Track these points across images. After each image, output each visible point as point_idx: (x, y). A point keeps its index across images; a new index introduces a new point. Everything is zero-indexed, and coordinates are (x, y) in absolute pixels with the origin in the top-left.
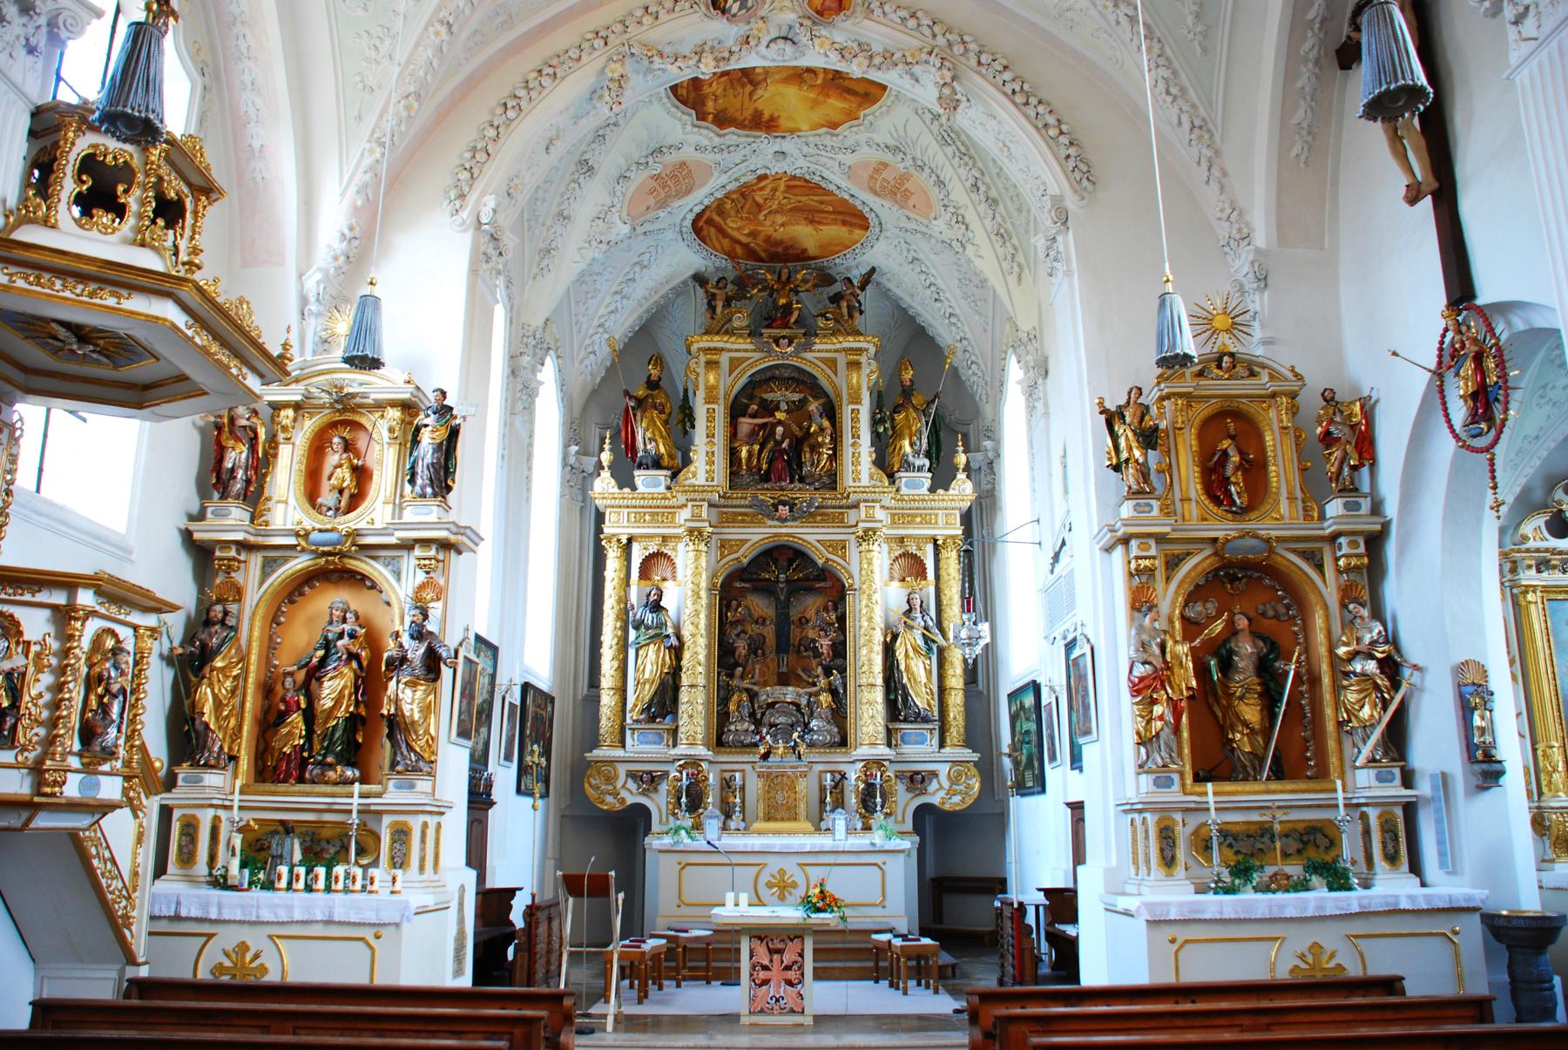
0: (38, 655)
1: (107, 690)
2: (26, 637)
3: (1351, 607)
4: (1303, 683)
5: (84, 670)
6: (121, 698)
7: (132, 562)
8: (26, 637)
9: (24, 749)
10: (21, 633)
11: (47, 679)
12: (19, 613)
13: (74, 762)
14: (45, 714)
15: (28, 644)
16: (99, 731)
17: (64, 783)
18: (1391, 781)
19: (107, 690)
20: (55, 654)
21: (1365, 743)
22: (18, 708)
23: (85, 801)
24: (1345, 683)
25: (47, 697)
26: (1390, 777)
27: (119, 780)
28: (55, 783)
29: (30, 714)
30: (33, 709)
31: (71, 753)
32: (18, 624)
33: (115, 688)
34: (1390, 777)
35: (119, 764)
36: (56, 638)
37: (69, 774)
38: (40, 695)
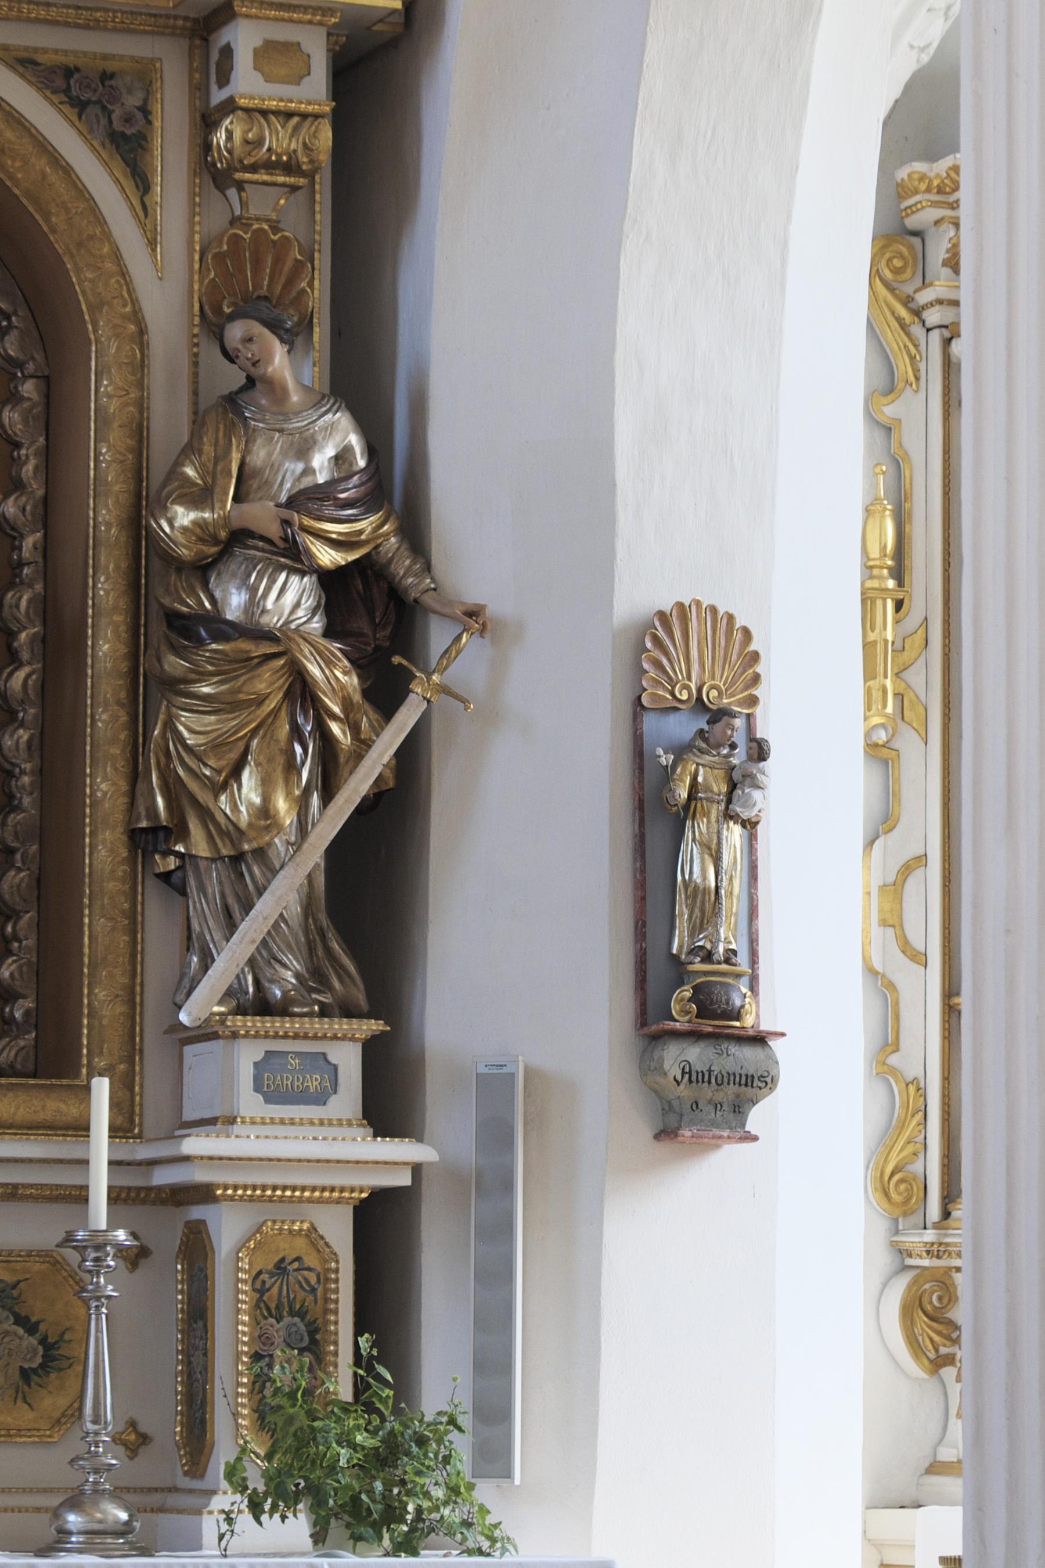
3: (235, 331)
4: (14, 659)
18: (320, 1099)
21: (231, 926)
24: (174, 664)
26: (314, 1082)
34: (314, 1082)
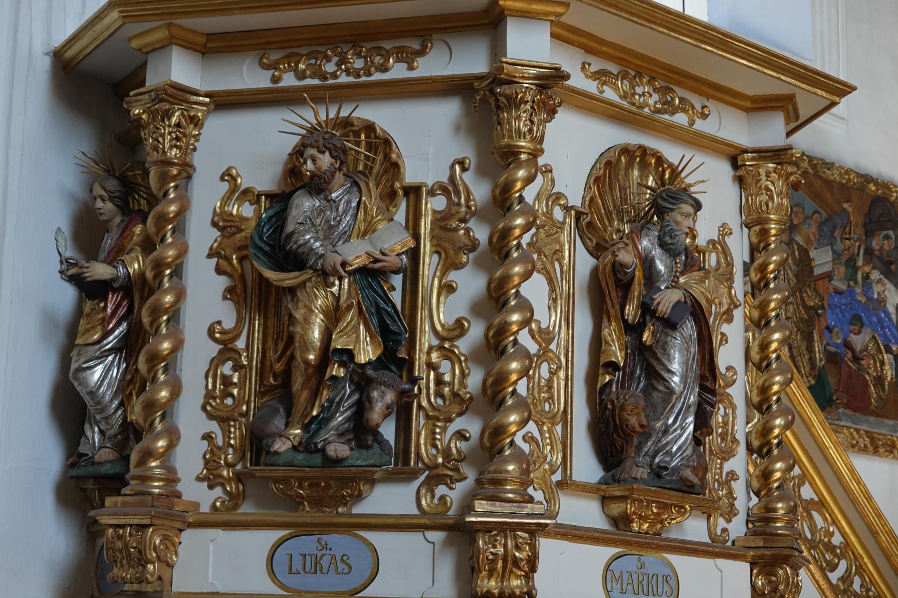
0: (441, 220)
1: (647, 309)
2: (410, 177)
5: (584, 263)
6: (689, 328)
8: (410, 177)
9: (435, 479)
10: (394, 168)
14: (475, 380)
15: (414, 192)
16: (633, 421)
17: (533, 569)
19: (647, 309)
22: (409, 364)
25: (476, 332)
27: (741, 570)
30: (445, 367)
35: (737, 528)
36: (483, 171)
37: (546, 545)
38: (459, 328)
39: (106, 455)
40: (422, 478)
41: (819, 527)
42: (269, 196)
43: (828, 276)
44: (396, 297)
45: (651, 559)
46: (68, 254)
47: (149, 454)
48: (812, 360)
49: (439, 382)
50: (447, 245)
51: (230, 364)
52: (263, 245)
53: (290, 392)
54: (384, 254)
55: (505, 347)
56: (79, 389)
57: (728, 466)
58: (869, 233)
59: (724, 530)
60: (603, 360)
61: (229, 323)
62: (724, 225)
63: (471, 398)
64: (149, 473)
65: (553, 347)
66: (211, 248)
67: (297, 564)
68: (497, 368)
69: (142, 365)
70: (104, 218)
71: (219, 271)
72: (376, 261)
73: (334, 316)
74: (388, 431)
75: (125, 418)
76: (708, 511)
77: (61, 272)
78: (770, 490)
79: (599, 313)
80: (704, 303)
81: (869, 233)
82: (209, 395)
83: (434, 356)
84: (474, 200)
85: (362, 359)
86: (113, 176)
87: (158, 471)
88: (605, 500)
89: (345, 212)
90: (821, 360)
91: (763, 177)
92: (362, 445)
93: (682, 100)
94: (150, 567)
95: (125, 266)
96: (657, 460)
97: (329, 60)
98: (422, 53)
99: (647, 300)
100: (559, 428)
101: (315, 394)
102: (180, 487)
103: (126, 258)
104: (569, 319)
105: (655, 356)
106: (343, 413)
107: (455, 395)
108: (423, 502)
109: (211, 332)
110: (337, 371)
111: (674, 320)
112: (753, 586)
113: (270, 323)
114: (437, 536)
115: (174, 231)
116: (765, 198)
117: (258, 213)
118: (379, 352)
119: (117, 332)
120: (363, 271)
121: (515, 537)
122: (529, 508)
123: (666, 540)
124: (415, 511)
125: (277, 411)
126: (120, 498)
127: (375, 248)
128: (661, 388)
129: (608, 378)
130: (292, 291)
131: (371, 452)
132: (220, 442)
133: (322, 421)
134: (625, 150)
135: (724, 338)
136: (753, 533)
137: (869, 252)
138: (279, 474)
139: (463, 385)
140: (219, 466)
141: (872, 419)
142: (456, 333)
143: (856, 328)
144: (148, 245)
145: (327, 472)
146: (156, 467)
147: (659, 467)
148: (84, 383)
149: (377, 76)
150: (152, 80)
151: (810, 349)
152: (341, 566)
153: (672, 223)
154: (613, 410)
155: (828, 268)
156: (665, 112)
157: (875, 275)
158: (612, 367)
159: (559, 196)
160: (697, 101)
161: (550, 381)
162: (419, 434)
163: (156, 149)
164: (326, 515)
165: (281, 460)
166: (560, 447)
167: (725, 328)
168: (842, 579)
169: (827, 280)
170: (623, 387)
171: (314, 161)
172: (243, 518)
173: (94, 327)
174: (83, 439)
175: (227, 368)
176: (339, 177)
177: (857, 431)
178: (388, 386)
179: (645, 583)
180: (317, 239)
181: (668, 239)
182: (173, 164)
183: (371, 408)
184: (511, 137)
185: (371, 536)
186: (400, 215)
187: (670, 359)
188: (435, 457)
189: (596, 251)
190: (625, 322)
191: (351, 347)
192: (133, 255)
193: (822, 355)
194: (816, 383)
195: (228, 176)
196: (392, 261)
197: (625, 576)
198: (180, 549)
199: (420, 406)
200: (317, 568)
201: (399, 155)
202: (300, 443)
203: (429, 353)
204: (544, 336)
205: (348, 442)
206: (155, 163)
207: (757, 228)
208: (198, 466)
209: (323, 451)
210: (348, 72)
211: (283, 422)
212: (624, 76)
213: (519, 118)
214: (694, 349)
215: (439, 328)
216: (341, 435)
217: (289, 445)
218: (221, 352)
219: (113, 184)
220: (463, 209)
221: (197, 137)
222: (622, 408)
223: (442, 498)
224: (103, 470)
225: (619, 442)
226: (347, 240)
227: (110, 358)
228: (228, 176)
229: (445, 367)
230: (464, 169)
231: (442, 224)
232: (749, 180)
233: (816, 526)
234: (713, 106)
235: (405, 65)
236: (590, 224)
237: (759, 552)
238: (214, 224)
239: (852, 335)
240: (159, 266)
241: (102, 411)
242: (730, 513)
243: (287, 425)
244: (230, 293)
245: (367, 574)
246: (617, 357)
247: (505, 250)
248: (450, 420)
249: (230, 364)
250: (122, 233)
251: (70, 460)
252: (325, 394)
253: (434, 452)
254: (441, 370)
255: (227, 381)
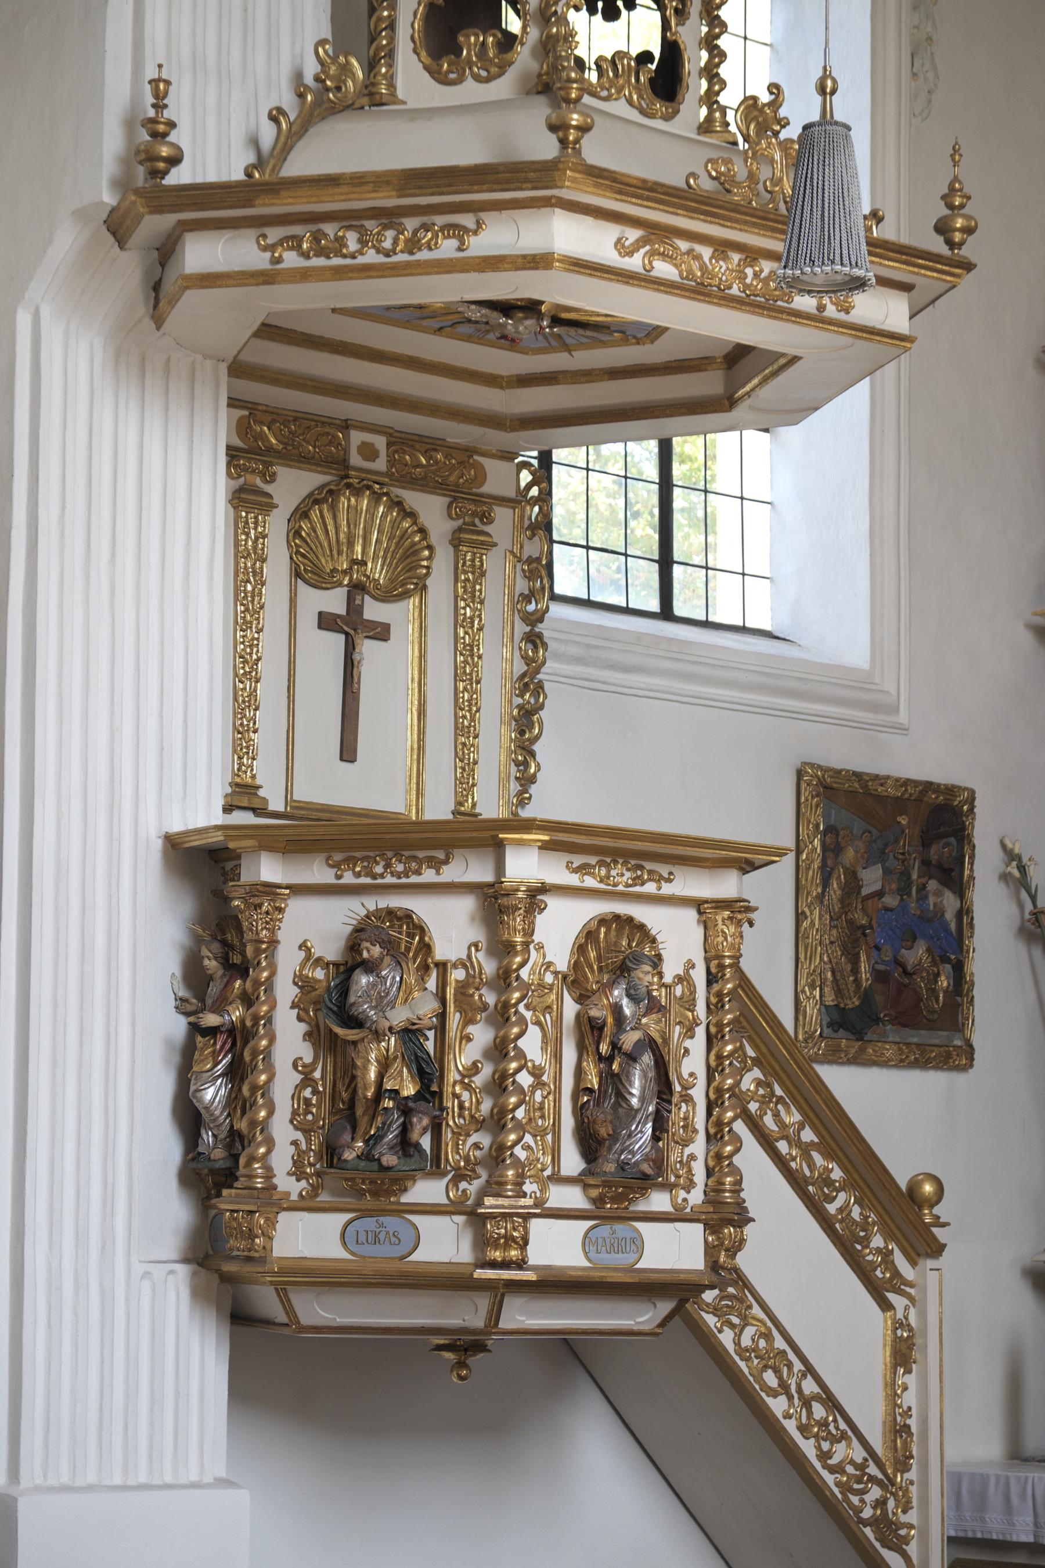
0: (462, 988)
1: (615, 1046)
2: (440, 953)
5: (570, 1008)
6: (647, 1059)
7: (902, 729)
8: (440, 953)
10: (426, 948)
11: (482, 1035)
12: (421, 907)
13: (572, 1197)
14: (486, 1106)
15: (442, 967)
16: (603, 1132)
17: (526, 1242)
19: (615, 1046)
20: (491, 985)
22: (440, 1094)
23: (596, 1275)
25: (487, 1071)
27: (697, 1230)
28: (509, 1240)
29: (461, 1107)
30: (465, 1096)
31: (557, 1178)
32: (421, 929)
33: (630, 1039)
35: (696, 1197)
37: (535, 1224)
38: (474, 1069)
39: (219, 1154)
40: (450, 1176)
41: (818, 1165)
42: (336, 965)
43: (879, 894)
44: (430, 1046)
45: (620, 1228)
46: (182, 993)
47: (252, 1159)
48: (857, 981)
49: (461, 1107)
50: (466, 1007)
51: (309, 1089)
52: (332, 1006)
53: (354, 1114)
54: (420, 1019)
55: (506, 1086)
56: (197, 1105)
57: (688, 1151)
58: (926, 844)
59: (685, 1200)
60: (582, 1086)
61: (308, 1059)
62: (690, 961)
63: (484, 1120)
64: (254, 1173)
65: (545, 1078)
66: (293, 1002)
67: (362, 1238)
68: (501, 1101)
69: (246, 1090)
70: (210, 972)
71: (300, 1019)
72: (414, 1024)
73: (384, 1065)
74: (426, 1142)
75: (232, 1126)
76: (669, 1187)
77: (177, 1008)
78: (722, 1167)
79: (581, 1048)
80: (659, 1041)
81: (926, 844)
82: (295, 1113)
83: (458, 1089)
84: (485, 974)
85: (405, 1093)
86: (216, 939)
87: (260, 1171)
88: (586, 1187)
89: (392, 985)
90: (867, 980)
91: (720, 922)
92: (406, 1155)
93: (650, 872)
94: (257, 1241)
95: (229, 1015)
96: (623, 1157)
97: (377, 863)
98: (446, 862)
99: (615, 1040)
100: (549, 1137)
101: (373, 1118)
102: (275, 1181)
103: (230, 1008)
104: (558, 1057)
105: (621, 1081)
106: (392, 1132)
107: (472, 1117)
108: (451, 1194)
109: (295, 1065)
110: (388, 1103)
111: (634, 1055)
112: (706, 1241)
113: (339, 1059)
114: (460, 1219)
115: (265, 991)
116: (721, 939)
117: (327, 975)
118: (417, 1088)
119: (224, 1062)
120: (406, 1031)
121: (513, 1222)
122: (523, 1202)
123: (633, 1212)
124: (446, 1201)
125: (345, 1128)
126: (233, 1191)
127: (413, 1013)
128: (624, 1105)
129: (585, 1099)
130: (354, 1043)
131: (413, 1159)
132: (304, 1147)
133: (378, 1138)
134: (603, 921)
135: (687, 1051)
136: (707, 1201)
137: (926, 863)
138: (348, 1176)
139: (478, 1110)
140: (303, 1165)
141: (923, 1032)
142: (473, 1072)
143: (909, 943)
144: (248, 1000)
145: (382, 1175)
146: (258, 1168)
147: (623, 1162)
148: (200, 1100)
149: (414, 879)
150: (246, 877)
151: (855, 971)
152: (393, 1239)
153: (636, 979)
154: (589, 1124)
155: (878, 886)
156: (635, 885)
157: (932, 885)
158: (589, 1091)
159: (549, 964)
160: (664, 870)
161: (542, 1103)
162: (447, 1145)
163: (251, 930)
164: (383, 1203)
165: (349, 1166)
166: (550, 1151)
167: (688, 1043)
168: (840, 1210)
169: (876, 899)
170: (598, 1105)
171: (368, 951)
172: (323, 1205)
173: (207, 1058)
174: (200, 1141)
175: (307, 1093)
176: (387, 960)
177: (908, 1044)
178: (424, 1113)
179: (616, 1245)
180: (372, 1008)
181: (632, 992)
182: (264, 942)
183: (412, 1130)
184: (509, 933)
185: (413, 1218)
186: (432, 984)
187: (631, 1085)
188: (459, 1161)
189: (581, 999)
190: (599, 1054)
191: (397, 1088)
192: (234, 1005)
193: (868, 975)
194: (861, 1003)
195: (303, 946)
196: (426, 1022)
197: (600, 1241)
198: (278, 1226)
199: (448, 1124)
200: (376, 1240)
201: (430, 938)
202: (362, 1153)
203: (454, 1086)
204: (536, 1073)
205: (396, 1153)
206: (251, 941)
207: (716, 962)
208: (289, 1164)
209: (379, 1160)
210: (392, 874)
211: (350, 1136)
212: (601, 863)
213: (515, 920)
214: (651, 1074)
215: (461, 1068)
216: (391, 1148)
217: (354, 1154)
218: (302, 1080)
219: (216, 947)
220: (478, 980)
221: (280, 921)
222: (594, 1122)
223: (464, 1191)
224: (217, 1165)
225: (594, 1145)
226: (393, 1007)
227: (220, 1081)
228: (303, 946)
229: (465, 1096)
230: (477, 950)
231: (463, 991)
232: (709, 924)
233: (814, 1164)
234: (677, 870)
235: (434, 871)
236: (573, 982)
237: (709, 1216)
238: (295, 984)
239: (903, 951)
240: (256, 1019)
241: (215, 1120)
242: (690, 1186)
243: (353, 1139)
244: (308, 1036)
245: (412, 1245)
246: (592, 1084)
247: (506, 1015)
248: (468, 1135)
249: (309, 1089)
250: (226, 986)
251: (191, 1156)
252: (380, 1119)
253: (458, 1157)
254: (463, 1099)
255: (307, 1102)
